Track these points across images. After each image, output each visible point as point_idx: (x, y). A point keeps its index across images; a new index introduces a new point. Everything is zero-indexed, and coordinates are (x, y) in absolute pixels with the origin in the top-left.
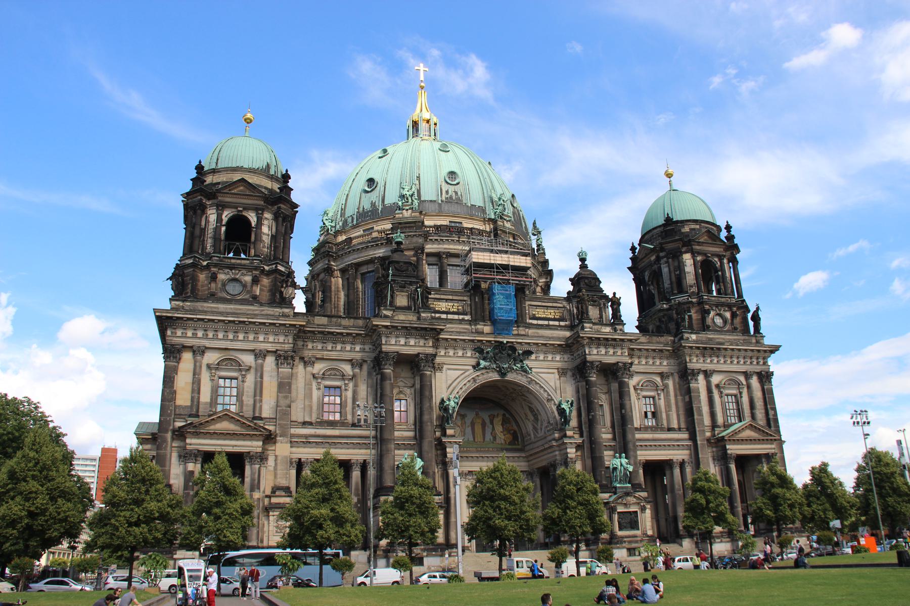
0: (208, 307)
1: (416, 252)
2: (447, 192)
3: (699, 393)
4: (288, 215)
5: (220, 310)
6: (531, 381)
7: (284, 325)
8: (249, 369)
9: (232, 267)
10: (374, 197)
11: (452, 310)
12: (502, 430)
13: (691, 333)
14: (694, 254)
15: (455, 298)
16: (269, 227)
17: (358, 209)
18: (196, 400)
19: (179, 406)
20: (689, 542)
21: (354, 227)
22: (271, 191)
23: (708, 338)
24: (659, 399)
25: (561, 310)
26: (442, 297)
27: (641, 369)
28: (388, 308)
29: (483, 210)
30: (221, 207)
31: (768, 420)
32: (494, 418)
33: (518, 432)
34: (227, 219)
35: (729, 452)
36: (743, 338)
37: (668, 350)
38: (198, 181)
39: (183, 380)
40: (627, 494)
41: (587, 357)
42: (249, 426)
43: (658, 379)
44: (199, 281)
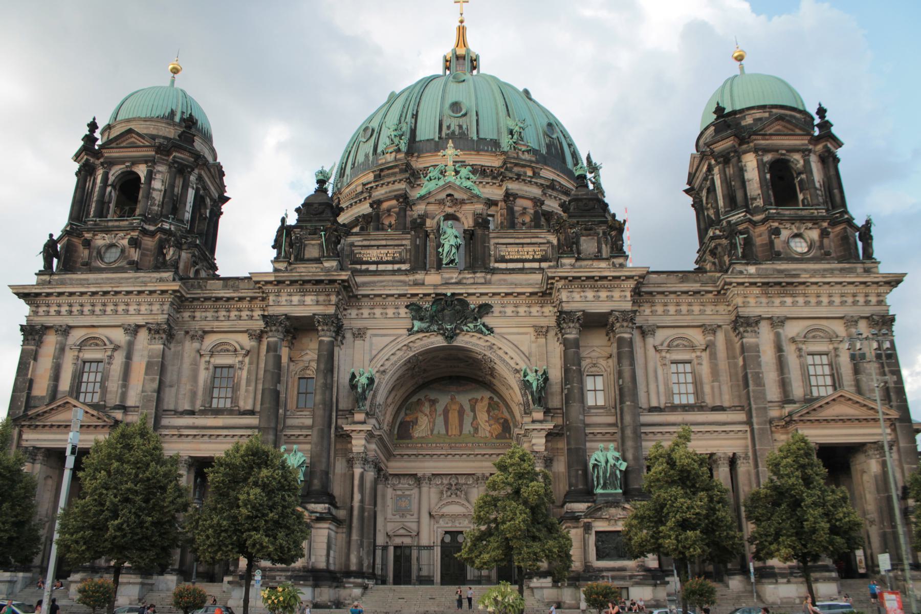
0: (77, 279)
1: (398, 200)
2: (449, 127)
3: (759, 352)
4: (186, 165)
5: (89, 282)
6: (491, 347)
7: (155, 292)
8: (116, 348)
9: (107, 231)
10: (368, 147)
12: (487, 419)
13: (747, 264)
14: (756, 150)
16: (163, 181)
17: (354, 164)
18: (50, 389)
19: (35, 397)
20: (740, 581)
21: (349, 185)
24: (700, 364)
25: (544, 247)
26: (373, 243)
27: (667, 321)
28: (281, 259)
29: (496, 144)
32: (476, 403)
33: (510, 421)
34: (113, 178)
37: (711, 292)
38: (89, 140)
39: (45, 365)
40: (615, 504)
41: (564, 305)
42: (93, 415)
43: (697, 337)
44: (76, 251)
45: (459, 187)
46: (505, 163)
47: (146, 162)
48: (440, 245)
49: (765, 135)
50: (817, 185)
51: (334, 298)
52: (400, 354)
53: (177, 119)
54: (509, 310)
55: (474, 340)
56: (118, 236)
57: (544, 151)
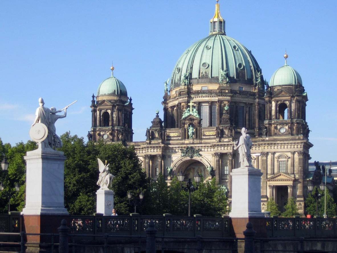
2: (202, 73)
10: (178, 77)
11: (175, 136)
13: (266, 137)
15: (176, 131)
17: (175, 81)
22: (116, 101)
23: (274, 138)
24: (254, 163)
26: (172, 131)
29: (217, 78)
30: (100, 110)
31: (298, 171)
35: (271, 184)
36: (291, 137)
37: (257, 144)
38: (93, 101)
45: (193, 116)
46: (218, 89)
47: (110, 109)
48: (188, 132)
49: (277, 97)
50: (292, 111)
51: (161, 150)
52: (179, 162)
53: (116, 94)
54: (206, 150)
55: (197, 158)
56: (106, 132)
57: (235, 78)
